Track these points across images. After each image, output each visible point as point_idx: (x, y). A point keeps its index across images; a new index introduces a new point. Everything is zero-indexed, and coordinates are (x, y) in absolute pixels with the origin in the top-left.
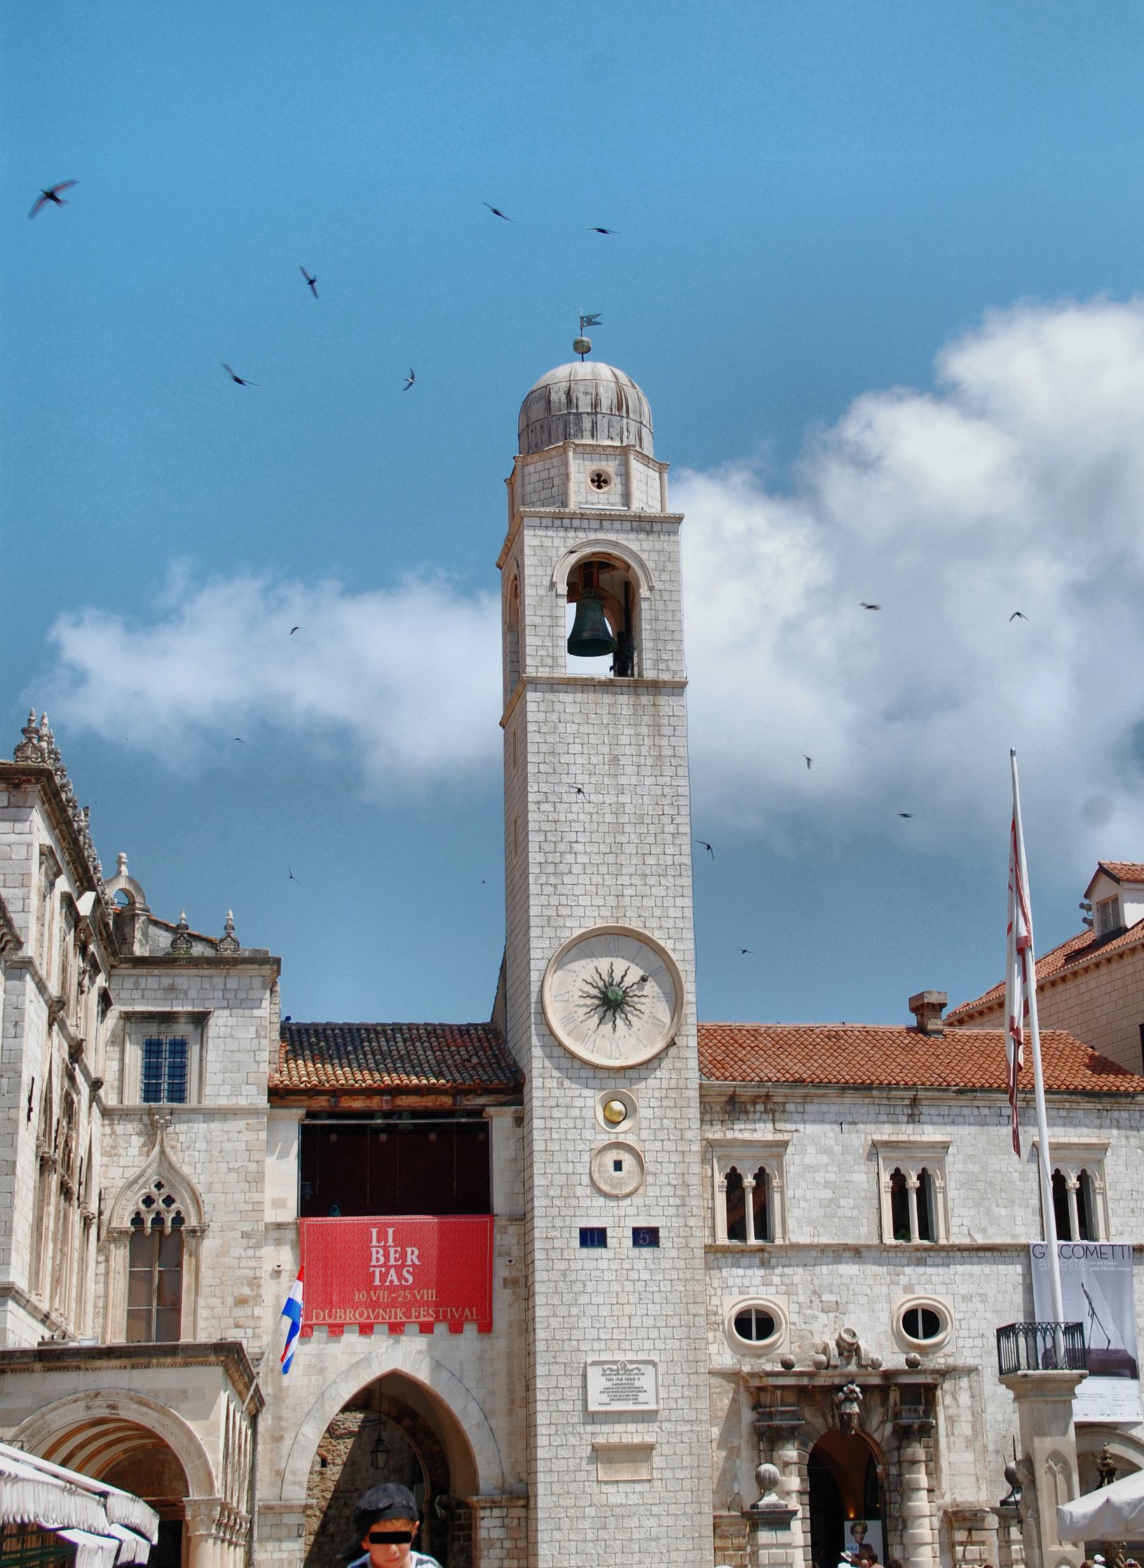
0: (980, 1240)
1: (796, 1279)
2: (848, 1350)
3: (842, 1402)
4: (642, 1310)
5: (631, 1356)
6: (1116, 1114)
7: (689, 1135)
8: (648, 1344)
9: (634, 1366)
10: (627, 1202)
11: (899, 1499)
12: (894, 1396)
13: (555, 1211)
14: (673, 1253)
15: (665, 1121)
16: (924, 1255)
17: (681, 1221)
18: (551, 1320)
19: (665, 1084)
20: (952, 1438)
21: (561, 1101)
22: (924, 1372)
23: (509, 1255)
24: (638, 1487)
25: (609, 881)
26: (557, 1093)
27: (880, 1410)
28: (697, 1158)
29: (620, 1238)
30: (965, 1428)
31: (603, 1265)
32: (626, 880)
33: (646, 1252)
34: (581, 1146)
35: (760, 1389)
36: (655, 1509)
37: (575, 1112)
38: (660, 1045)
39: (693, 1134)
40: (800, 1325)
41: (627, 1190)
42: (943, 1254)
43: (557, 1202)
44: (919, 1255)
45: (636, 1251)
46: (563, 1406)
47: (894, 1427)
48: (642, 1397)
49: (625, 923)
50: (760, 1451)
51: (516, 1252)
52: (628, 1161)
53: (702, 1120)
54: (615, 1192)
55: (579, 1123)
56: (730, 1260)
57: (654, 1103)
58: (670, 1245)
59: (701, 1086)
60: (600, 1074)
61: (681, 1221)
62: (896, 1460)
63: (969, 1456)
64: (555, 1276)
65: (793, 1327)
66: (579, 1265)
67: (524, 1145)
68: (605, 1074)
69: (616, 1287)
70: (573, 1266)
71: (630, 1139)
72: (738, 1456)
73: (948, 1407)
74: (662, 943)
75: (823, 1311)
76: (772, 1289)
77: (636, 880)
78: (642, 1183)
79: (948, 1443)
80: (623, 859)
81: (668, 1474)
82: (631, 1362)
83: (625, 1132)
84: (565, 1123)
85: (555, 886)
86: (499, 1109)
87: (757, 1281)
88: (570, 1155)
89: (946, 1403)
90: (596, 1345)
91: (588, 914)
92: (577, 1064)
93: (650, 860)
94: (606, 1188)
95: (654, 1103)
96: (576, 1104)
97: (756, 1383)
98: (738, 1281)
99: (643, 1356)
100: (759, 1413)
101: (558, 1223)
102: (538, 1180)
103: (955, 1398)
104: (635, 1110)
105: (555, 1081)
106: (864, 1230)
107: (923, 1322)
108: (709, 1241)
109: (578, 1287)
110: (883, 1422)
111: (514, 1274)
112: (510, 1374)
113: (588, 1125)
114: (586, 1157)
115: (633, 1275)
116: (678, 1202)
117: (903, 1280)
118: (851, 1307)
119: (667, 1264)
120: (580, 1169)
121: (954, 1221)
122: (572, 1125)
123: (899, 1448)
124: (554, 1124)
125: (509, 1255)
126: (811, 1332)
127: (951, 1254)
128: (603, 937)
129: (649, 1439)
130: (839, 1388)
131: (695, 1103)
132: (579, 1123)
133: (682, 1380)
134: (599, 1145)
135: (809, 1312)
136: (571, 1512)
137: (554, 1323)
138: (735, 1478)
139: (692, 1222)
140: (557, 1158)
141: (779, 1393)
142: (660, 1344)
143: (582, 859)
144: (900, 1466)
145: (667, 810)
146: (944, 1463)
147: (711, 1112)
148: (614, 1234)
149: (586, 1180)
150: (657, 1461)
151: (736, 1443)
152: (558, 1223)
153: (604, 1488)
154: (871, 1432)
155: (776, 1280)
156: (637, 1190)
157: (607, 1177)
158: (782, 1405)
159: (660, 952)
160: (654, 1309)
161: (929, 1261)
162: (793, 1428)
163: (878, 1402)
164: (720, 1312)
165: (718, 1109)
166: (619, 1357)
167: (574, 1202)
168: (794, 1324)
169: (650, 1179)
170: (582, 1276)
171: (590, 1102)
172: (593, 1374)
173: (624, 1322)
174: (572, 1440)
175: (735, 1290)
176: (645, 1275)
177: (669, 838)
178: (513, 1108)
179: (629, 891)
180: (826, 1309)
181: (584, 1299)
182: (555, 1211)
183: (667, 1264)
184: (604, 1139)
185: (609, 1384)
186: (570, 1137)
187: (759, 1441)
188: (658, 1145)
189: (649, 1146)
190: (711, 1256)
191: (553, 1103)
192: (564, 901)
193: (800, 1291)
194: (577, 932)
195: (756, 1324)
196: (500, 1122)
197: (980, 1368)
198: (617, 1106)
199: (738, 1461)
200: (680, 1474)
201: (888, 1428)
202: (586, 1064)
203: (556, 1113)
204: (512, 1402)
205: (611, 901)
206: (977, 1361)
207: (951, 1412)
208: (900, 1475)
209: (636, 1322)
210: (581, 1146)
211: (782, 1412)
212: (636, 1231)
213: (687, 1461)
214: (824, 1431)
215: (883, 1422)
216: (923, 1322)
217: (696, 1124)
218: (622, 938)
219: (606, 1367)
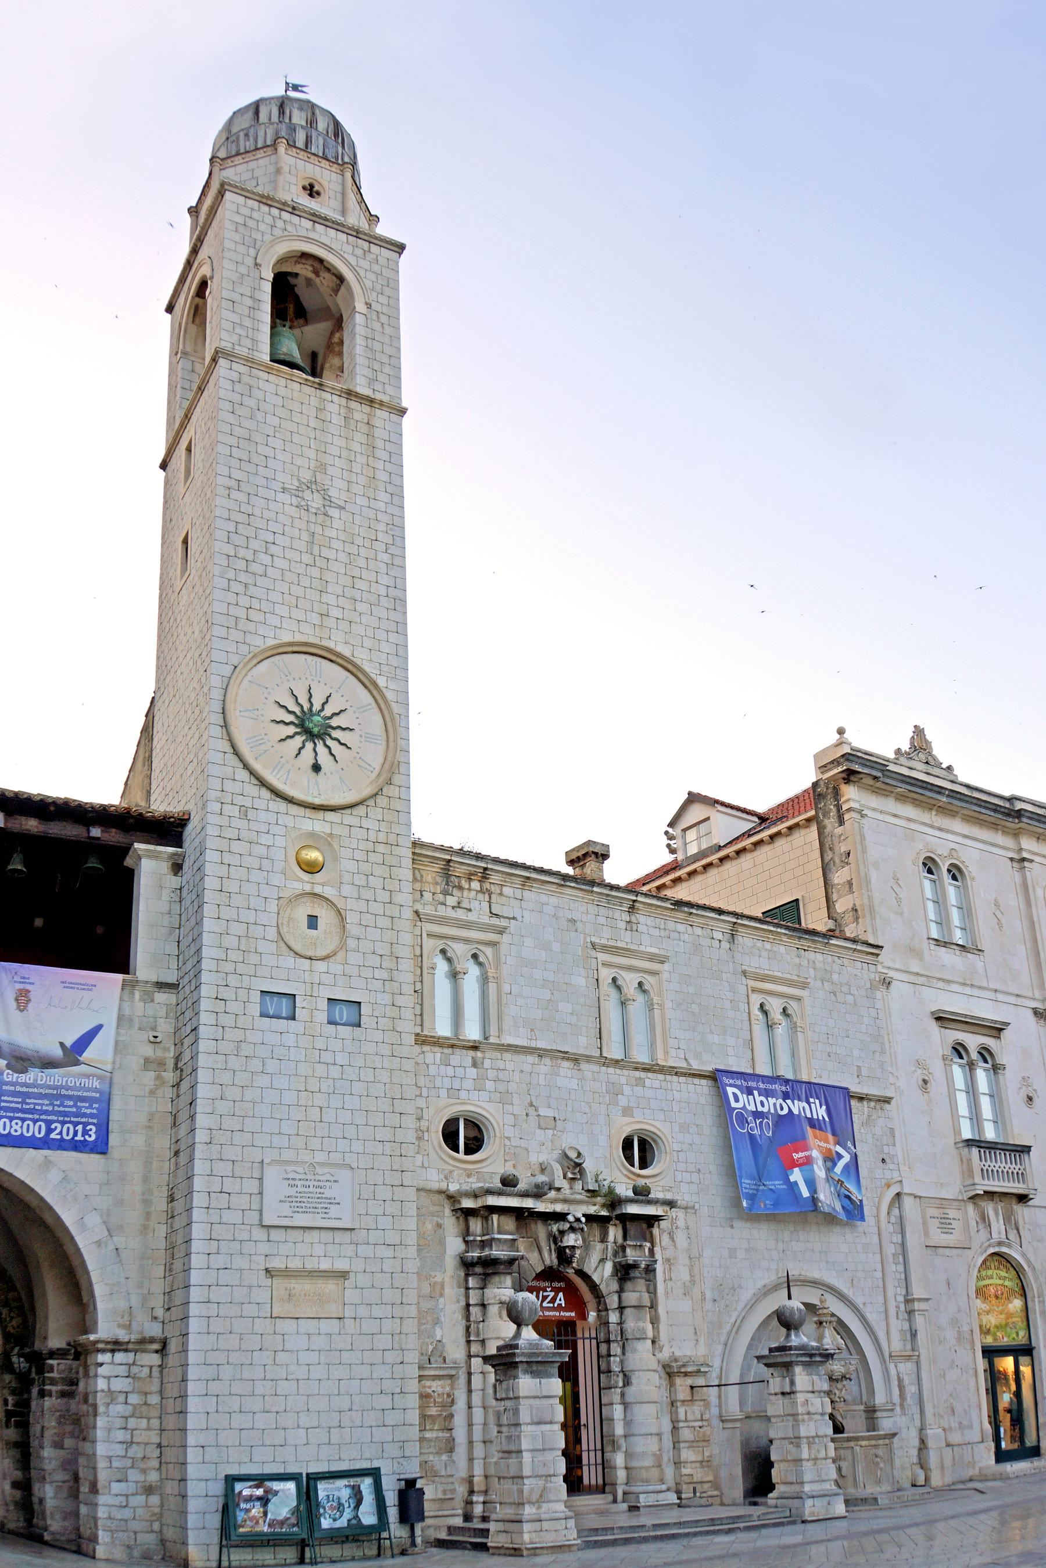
0: (696, 1065)
1: (512, 1087)
2: (575, 1167)
3: (562, 1233)
4: (336, 1102)
5: (320, 1157)
6: (811, 955)
7: (399, 898)
8: (343, 1145)
9: (326, 1170)
10: (321, 966)
11: (619, 1351)
12: (614, 1233)
13: (229, 967)
14: (378, 1036)
15: (370, 877)
16: (643, 1075)
17: (386, 999)
18: (218, 1103)
19: (372, 836)
20: (670, 1283)
21: (244, 834)
22: (655, 1202)
24: (325, 1326)
25: (313, 595)
26: (237, 823)
27: (599, 1246)
28: (407, 925)
29: (312, 1010)
30: (682, 1273)
31: (290, 1040)
32: (331, 599)
33: (344, 1031)
34: (266, 891)
35: (468, 1213)
36: (346, 1357)
37: (261, 851)
39: (404, 898)
40: (515, 1142)
41: (321, 953)
42: (661, 1077)
43: (232, 956)
44: (637, 1074)
46: (228, 1216)
47: (615, 1266)
48: (334, 1211)
50: (467, 1289)
54: (309, 954)
55: (266, 864)
56: (438, 1055)
60: (294, 810)
61: (386, 999)
62: (616, 1306)
63: (686, 1305)
64: (226, 1047)
65: (507, 1142)
66: (256, 1037)
68: (301, 811)
69: (304, 1069)
70: (251, 1036)
71: (329, 892)
72: (441, 1295)
73: (665, 1249)
75: (540, 1127)
76: (484, 1095)
77: (342, 601)
78: (343, 945)
79: (666, 1288)
80: (328, 576)
81: (363, 1311)
82: (322, 1164)
84: (247, 861)
87: (468, 1084)
88: (252, 900)
89: (663, 1244)
90: (277, 1141)
91: (284, 625)
92: (265, 794)
93: (359, 584)
94: (298, 948)
95: (359, 855)
96: (262, 841)
97: (467, 1203)
98: (447, 1083)
99: (335, 1158)
100: (466, 1242)
101: (233, 980)
103: (672, 1239)
104: (336, 858)
106: (583, 1040)
107: (640, 1150)
108: (418, 1030)
109: (256, 1065)
110: (602, 1260)
111: (159, 1053)
112: (146, 1179)
113: (278, 866)
114: (273, 907)
115: (327, 1057)
116: (385, 975)
117: (623, 1101)
118: (569, 1125)
119: (369, 1048)
120: (263, 918)
121: (672, 1043)
122: (257, 866)
123: (621, 1291)
124: (234, 860)
126: (527, 1150)
127: (668, 1077)
129: (341, 1265)
130: (561, 1217)
132: (266, 864)
133: (385, 1193)
134: (286, 894)
135: (524, 1126)
136: (235, 1357)
137: (223, 1107)
138: (437, 1322)
139: (400, 1001)
140: (236, 900)
141: (495, 1217)
142: (357, 1146)
143: (285, 565)
144: (621, 1314)
145: (381, 536)
146: (661, 1310)
147: (421, 881)
148: (304, 1004)
149: (272, 934)
150: (351, 1295)
151: (439, 1279)
152: (233, 980)
153: (286, 1326)
154: (590, 1273)
155: (490, 1085)
157: (299, 934)
158: (499, 1233)
159: (369, 685)
160: (351, 1102)
161: (648, 1082)
162: (511, 1261)
163: (597, 1238)
164: (425, 1117)
166: (305, 1156)
167: (254, 958)
168: (509, 1138)
169: (352, 943)
170: (263, 1052)
171: (280, 842)
172: (272, 1176)
173: (314, 1113)
174: (239, 1262)
175: (443, 1093)
176: (341, 1059)
177: (383, 566)
180: (543, 1125)
181: (262, 1081)
182: (229, 967)
183: (369, 1048)
184: (298, 887)
185: (292, 1191)
186: (252, 878)
187: (467, 1275)
188: (362, 906)
189: (351, 904)
193: (516, 1100)
195: (464, 1136)
197: (697, 1206)
199: (441, 1300)
200: (378, 1311)
201: (608, 1268)
203: (236, 846)
204: (148, 1215)
205: (315, 619)
206: (695, 1198)
207: (668, 1254)
208: (621, 1323)
209: (329, 1116)
210: (266, 891)
211: (499, 1240)
213: (389, 1296)
214: (539, 1268)
215: (602, 1260)
216: (640, 1150)
219: (289, 1169)
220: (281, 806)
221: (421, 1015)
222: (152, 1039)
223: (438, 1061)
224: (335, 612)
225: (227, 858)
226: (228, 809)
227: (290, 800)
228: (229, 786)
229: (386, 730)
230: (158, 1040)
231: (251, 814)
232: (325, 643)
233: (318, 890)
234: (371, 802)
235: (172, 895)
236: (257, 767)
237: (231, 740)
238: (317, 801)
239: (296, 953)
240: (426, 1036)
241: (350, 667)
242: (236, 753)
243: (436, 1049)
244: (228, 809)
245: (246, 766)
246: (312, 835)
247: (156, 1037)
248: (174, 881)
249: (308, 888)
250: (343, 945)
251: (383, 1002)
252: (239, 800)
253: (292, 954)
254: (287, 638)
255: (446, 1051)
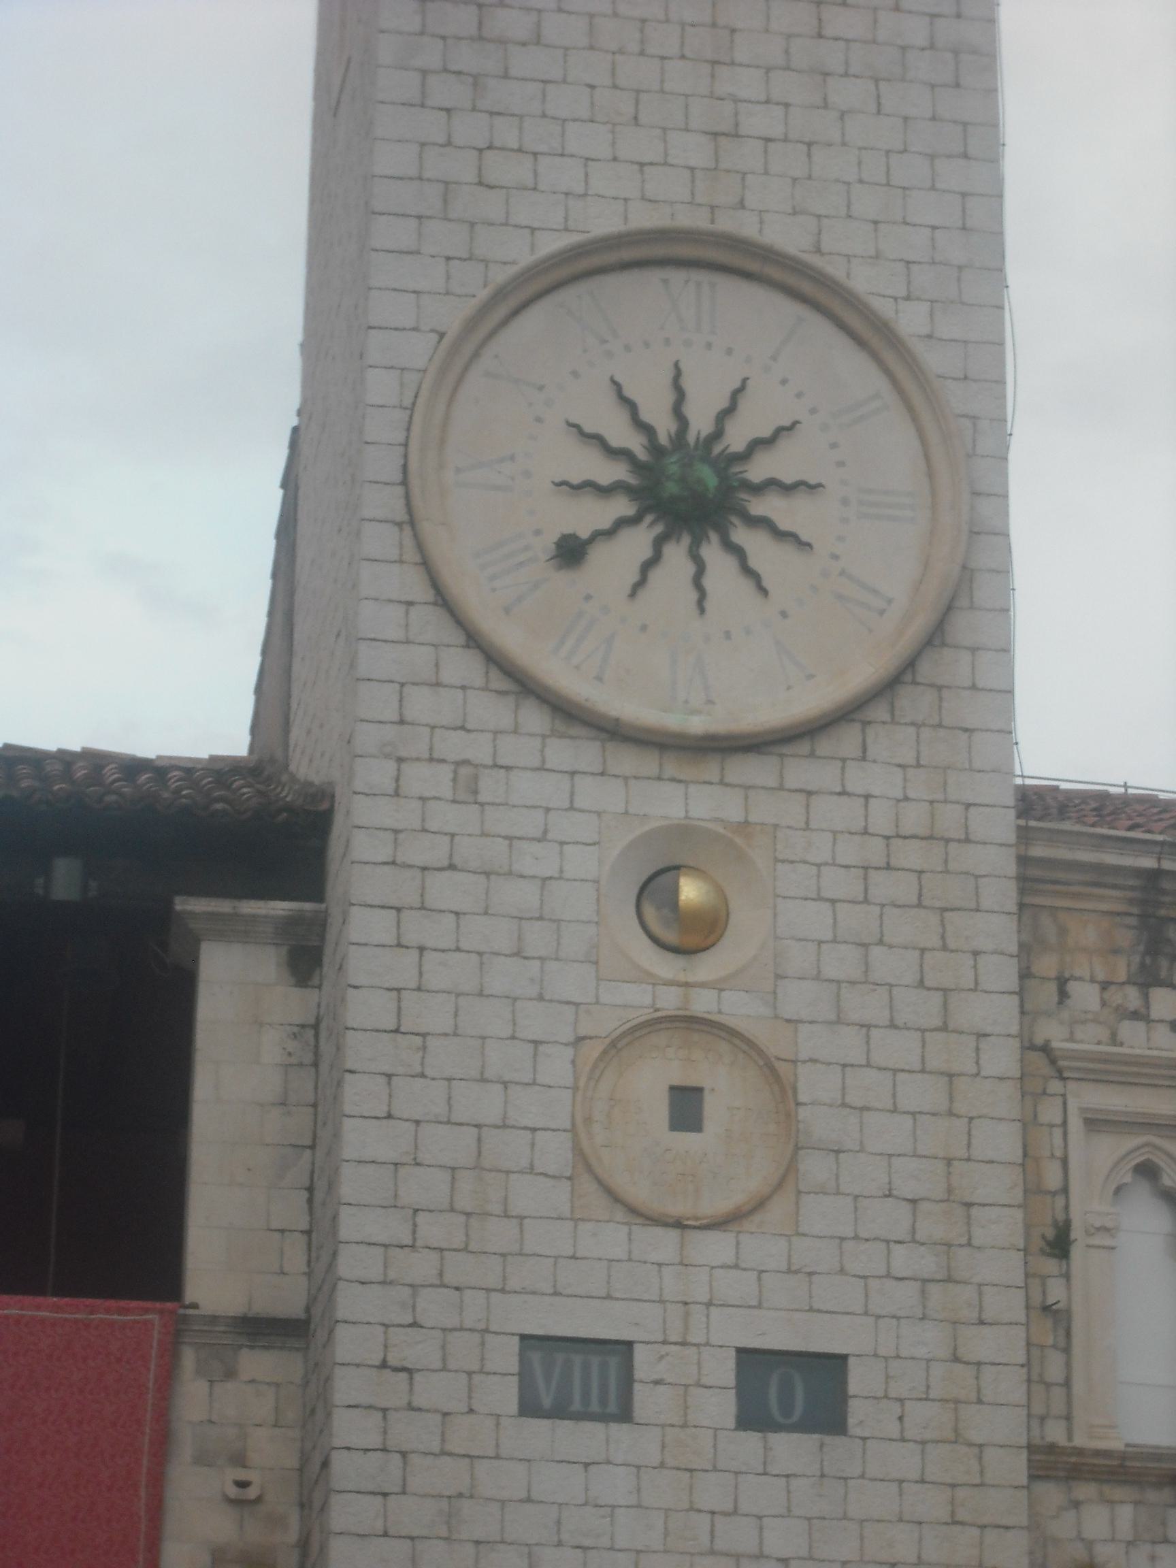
10: (715, 1248)
13: (421, 1267)
15: (876, 951)
19: (881, 819)
23: (239, 1460)
33: (792, 1450)
38: (863, 673)
39: (995, 1011)
41: (716, 1204)
43: (432, 1230)
45: (751, 1441)
49: (746, 226)
51: (271, 1453)
52: (727, 1090)
53: (1025, 975)
54: (676, 1208)
57: (839, 884)
58: (893, 1429)
59: (1025, 835)
60: (627, 760)
67: (317, 1045)
68: (648, 762)
71: (738, 1008)
74: (884, 308)
78: (787, 1177)
83: (719, 986)
85: (477, 81)
86: (224, 906)
92: (535, 718)
94: (640, 1192)
95: (839, 884)
101: (433, 1307)
102: (360, 1139)
105: (445, 772)
114: (557, 1066)
116: (927, 1264)
125: (239, 1460)
128: (654, 276)
131: (1001, 893)
134: (607, 1024)
139: (982, 1344)
149: (555, 1152)
156: (760, 1204)
165: (1088, 934)
169: (815, 1168)
178: (281, 908)
179: (759, 122)
182: (421, 1267)
184: (637, 1000)
190: (1052, 1494)
191: (429, 851)
192: (507, 134)
194: (551, 244)
196: (234, 991)
198: (690, 891)
202: (568, 714)
212: (747, 1357)
217: (1002, 973)
218: (728, 287)
220: (583, 752)
221: (1067, 1384)
222: (233, 1491)
223: (1125, 1527)
224: (759, 122)
225: (417, 929)
226: (420, 778)
227: (613, 732)
228: (421, 704)
229: (931, 474)
230: (252, 1493)
231: (490, 786)
232: (726, 224)
233: (703, 1003)
234: (879, 712)
235: (292, 1045)
236: (511, 638)
237: (426, 564)
238: (697, 725)
239: (633, 1210)
240: (1080, 1452)
241: (806, 287)
242: (443, 600)
243: (1118, 1493)
244: (420, 778)
245: (474, 640)
246: (684, 832)
247: (243, 1485)
248: (290, 1004)
249: (670, 1001)
250: (787, 1177)
251: (921, 1352)
252: (453, 746)
253: (620, 1215)
254: (603, 222)
255: (1152, 1495)
